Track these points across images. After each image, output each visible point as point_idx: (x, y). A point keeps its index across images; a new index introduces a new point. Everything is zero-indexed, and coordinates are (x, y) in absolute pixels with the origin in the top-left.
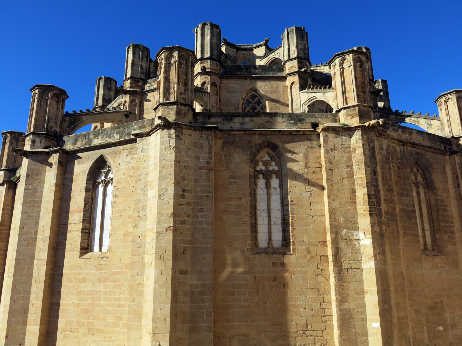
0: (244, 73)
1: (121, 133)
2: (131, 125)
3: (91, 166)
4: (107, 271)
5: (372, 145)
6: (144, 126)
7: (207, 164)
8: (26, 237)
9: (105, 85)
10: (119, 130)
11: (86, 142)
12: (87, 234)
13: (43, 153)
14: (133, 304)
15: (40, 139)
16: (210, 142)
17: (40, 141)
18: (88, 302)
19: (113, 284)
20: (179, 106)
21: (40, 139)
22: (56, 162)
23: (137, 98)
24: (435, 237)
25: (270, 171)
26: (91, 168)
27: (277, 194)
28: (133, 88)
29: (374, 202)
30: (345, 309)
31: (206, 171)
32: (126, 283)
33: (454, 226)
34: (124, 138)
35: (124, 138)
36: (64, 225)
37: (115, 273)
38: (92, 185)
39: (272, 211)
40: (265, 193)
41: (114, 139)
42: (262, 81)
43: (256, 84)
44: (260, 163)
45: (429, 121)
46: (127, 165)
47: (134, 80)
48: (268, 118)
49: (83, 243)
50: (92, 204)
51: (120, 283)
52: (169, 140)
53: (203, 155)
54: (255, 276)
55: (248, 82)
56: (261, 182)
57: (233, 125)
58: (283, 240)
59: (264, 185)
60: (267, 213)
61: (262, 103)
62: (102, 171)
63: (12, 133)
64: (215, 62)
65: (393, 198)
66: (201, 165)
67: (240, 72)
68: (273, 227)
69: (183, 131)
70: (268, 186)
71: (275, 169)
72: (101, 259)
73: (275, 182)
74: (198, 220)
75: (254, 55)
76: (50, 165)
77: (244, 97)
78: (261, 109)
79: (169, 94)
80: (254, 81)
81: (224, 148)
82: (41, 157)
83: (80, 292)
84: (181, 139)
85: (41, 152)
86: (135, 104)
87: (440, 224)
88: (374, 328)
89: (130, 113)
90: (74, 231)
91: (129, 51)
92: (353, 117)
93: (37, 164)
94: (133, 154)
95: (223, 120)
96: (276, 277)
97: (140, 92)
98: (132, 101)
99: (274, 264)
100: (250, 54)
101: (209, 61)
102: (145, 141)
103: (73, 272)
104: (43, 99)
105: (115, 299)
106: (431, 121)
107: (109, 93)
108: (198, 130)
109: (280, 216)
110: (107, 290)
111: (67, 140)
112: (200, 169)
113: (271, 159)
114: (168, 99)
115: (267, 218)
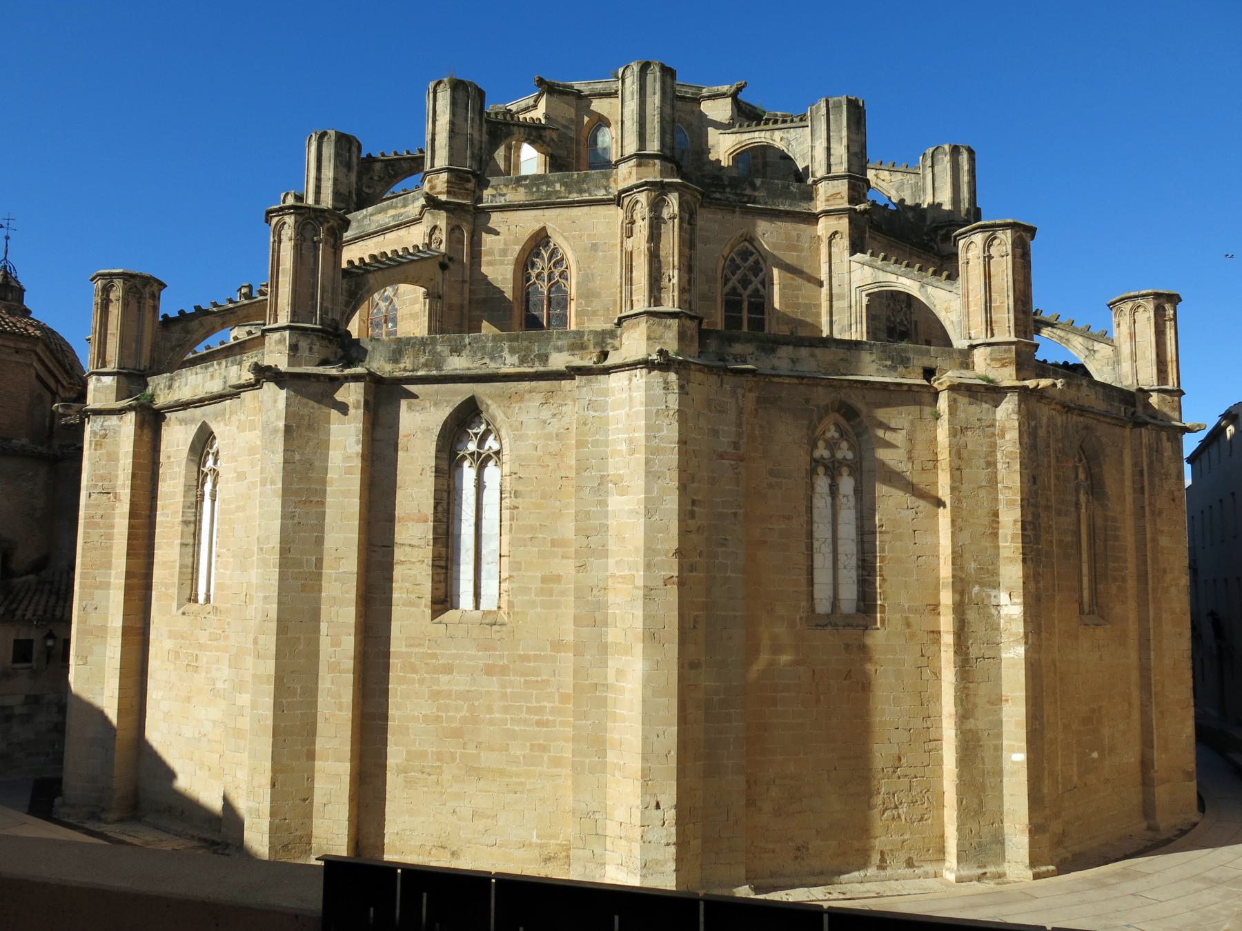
0: (728, 195)
1: (523, 353)
2: (547, 339)
3: (445, 418)
4: (505, 653)
5: (1033, 424)
6: (582, 344)
7: (735, 447)
8: (296, 570)
9: (337, 155)
10: (515, 344)
11: (427, 360)
12: (444, 571)
13: (322, 378)
14: (584, 722)
15: (309, 341)
16: (740, 401)
17: (308, 346)
18: (462, 714)
19: (522, 680)
20: (683, 319)
21: (309, 341)
22: (358, 402)
23: (464, 224)
24: (1096, 589)
25: (839, 462)
26: (445, 423)
27: (849, 508)
28: (455, 195)
29: (1029, 536)
30: (970, 730)
31: (733, 462)
32: (553, 679)
33: (1127, 568)
34: (531, 364)
35: (531, 364)
36: (384, 546)
37: (525, 658)
38: (447, 462)
39: (840, 542)
40: (829, 506)
41: (505, 364)
42: (767, 221)
43: (754, 225)
44: (821, 444)
45: (1090, 343)
46: (544, 428)
47: (457, 176)
48: (842, 350)
49: (437, 589)
50: (448, 504)
51: (539, 679)
52: (666, 394)
53: (726, 428)
54: (814, 671)
55: (737, 218)
56: (822, 483)
57: (776, 362)
58: (858, 600)
59: (826, 490)
60: (831, 547)
61: (762, 270)
62: (469, 431)
63: (126, 277)
64: (670, 165)
65: (1050, 523)
66: (723, 449)
67: (720, 193)
68: (842, 573)
69: (689, 375)
70: (834, 490)
71: (848, 458)
72: (489, 627)
73: (847, 484)
74: (717, 561)
75: (702, 116)
76: (343, 408)
77: (726, 252)
78: (761, 283)
79: (660, 289)
80: (750, 217)
81: (760, 410)
82: (316, 387)
83: (439, 692)
84: (687, 394)
85: (317, 377)
86: (460, 236)
87: (1107, 565)
88: (1014, 763)
89: (450, 259)
90: (413, 563)
91: (438, 94)
92: (1003, 366)
93: (307, 403)
94: (555, 405)
95: (757, 350)
96: (850, 671)
97: (471, 209)
98: (453, 230)
99: (847, 646)
100: (693, 112)
101: (657, 162)
102: (596, 386)
103: (416, 650)
104: (305, 240)
105: (529, 710)
106: (1096, 343)
107: (347, 176)
108: (716, 374)
109: (855, 552)
110: (509, 690)
111: (374, 349)
112: (721, 456)
113: (842, 436)
114: (658, 302)
115: (831, 555)
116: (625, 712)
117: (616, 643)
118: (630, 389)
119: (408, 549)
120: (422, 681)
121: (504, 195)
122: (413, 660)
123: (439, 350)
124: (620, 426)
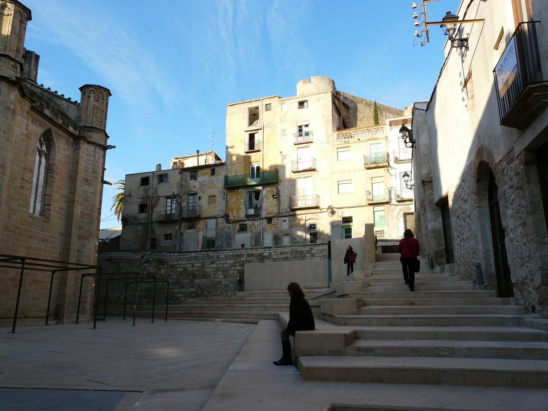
37: (52, 237)
90: (26, 189)
116: (84, 259)
117: (82, 236)
118: (95, 152)
119: (26, 182)
122: (22, 231)
123: (43, 104)
124: (90, 162)
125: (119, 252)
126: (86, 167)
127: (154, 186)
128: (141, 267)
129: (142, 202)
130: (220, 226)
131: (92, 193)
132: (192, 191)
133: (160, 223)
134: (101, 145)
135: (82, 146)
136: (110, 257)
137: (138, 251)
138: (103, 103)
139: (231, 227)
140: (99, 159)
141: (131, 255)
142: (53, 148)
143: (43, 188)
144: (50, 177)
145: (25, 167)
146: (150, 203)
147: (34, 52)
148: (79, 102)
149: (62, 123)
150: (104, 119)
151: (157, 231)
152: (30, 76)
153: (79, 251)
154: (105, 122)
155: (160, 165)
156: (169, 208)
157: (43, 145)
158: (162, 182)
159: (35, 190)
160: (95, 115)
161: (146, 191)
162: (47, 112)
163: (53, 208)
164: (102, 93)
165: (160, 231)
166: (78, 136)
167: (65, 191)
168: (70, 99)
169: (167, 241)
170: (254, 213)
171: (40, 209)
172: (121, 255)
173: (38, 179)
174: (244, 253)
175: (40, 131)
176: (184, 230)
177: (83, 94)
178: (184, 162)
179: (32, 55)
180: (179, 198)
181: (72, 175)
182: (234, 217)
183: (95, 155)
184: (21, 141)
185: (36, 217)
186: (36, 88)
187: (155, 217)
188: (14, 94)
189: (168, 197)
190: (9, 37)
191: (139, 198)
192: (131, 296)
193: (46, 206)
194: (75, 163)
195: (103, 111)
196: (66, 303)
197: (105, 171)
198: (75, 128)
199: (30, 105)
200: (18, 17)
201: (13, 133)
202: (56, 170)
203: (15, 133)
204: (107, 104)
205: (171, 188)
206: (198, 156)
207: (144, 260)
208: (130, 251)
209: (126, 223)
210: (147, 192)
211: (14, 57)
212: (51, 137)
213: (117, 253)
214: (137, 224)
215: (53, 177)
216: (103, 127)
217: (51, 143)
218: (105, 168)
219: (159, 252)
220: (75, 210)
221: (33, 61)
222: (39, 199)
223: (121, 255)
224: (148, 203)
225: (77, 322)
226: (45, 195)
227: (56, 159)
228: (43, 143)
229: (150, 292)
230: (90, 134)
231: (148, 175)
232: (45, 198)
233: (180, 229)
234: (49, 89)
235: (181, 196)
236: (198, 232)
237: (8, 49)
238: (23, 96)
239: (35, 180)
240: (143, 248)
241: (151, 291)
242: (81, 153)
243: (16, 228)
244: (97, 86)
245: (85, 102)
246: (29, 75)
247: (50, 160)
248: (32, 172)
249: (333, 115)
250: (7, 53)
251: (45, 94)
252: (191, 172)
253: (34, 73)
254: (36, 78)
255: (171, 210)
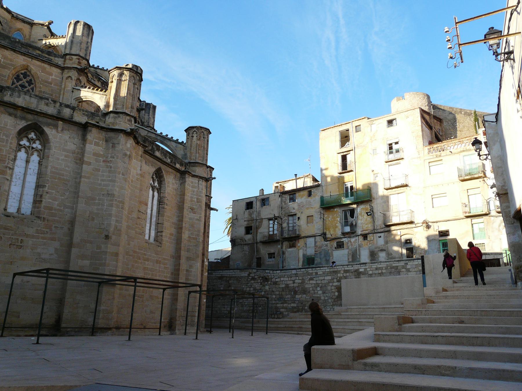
37: (164, 259)
51: (167, 266)
83: (145, 268)
90: (142, 219)
110: (161, 269)
116: (192, 278)
119: (141, 214)
120: (141, 263)
121: (95, 81)
124: (194, 193)
125: (229, 271)
126: (192, 197)
127: (257, 210)
128: (248, 283)
129: (248, 224)
130: (318, 244)
131: (197, 219)
132: (292, 212)
133: (264, 243)
134: (204, 177)
135: (187, 179)
136: (222, 275)
137: (246, 269)
138: (204, 140)
139: (329, 245)
140: (202, 189)
141: (239, 273)
142: (163, 183)
143: (156, 218)
144: (162, 208)
145: (141, 201)
146: (254, 225)
147: (152, 103)
148: (185, 142)
149: (170, 161)
150: (206, 155)
151: (262, 250)
152: (149, 124)
153: (187, 271)
154: (207, 157)
155: (262, 189)
156: (271, 229)
157: (155, 182)
158: (264, 205)
159: (149, 220)
160: (197, 152)
161: (250, 214)
162: (158, 154)
163: (164, 234)
164: (203, 132)
165: (264, 251)
166: (183, 171)
167: (175, 219)
168: (178, 140)
169: (271, 260)
170: (350, 231)
171: (154, 236)
172: (230, 273)
173: (152, 210)
174: (340, 269)
175: (152, 170)
176: (286, 249)
177: (188, 135)
178: (285, 185)
179: (150, 106)
180: (280, 219)
181: (180, 205)
182: (331, 235)
183: (198, 186)
184: (137, 180)
185: (151, 243)
186: (151, 134)
187: (259, 238)
188: (130, 143)
189: (270, 219)
190: (126, 98)
191: (245, 221)
192: (240, 311)
193: (159, 232)
194: (182, 195)
195: (204, 148)
196: (177, 317)
197: (212, 200)
198: (181, 165)
199: (143, 149)
200: (132, 81)
201: (130, 174)
202: (166, 201)
203: (132, 174)
204: (208, 141)
205: (272, 210)
206: (296, 179)
207: (250, 278)
208: (238, 269)
209: (234, 244)
210: (251, 215)
211: (129, 113)
212: (162, 174)
213: (226, 271)
214: (244, 245)
215: (164, 208)
216: (205, 162)
217: (162, 179)
218: (212, 196)
219: (263, 270)
220: (183, 235)
221: (151, 111)
222: (153, 227)
223: (230, 273)
224: (253, 225)
225: (185, 334)
226: (158, 223)
227: (166, 192)
228: (155, 180)
229: (256, 307)
230: (194, 168)
231: (251, 200)
232: (158, 226)
233: (282, 248)
234: (161, 133)
235: (282, 218)
236: (299, 250)
237: (125, 106)
238: (137, 143)
239: (149, 211)
240: (250, 267)
241: (258, 306)
242: (186, 186)
243: (135, 252)
244: (198, 127)
245: (189, 142)
246: (149, 123)
247: (161, 194)
248: (146, 205)
249: (422, 131)
250: (124, 110)
251: (159, 138)
252: (290, 195)
253: (152, 120)
254: (153, 125)
255: (273, 231)
